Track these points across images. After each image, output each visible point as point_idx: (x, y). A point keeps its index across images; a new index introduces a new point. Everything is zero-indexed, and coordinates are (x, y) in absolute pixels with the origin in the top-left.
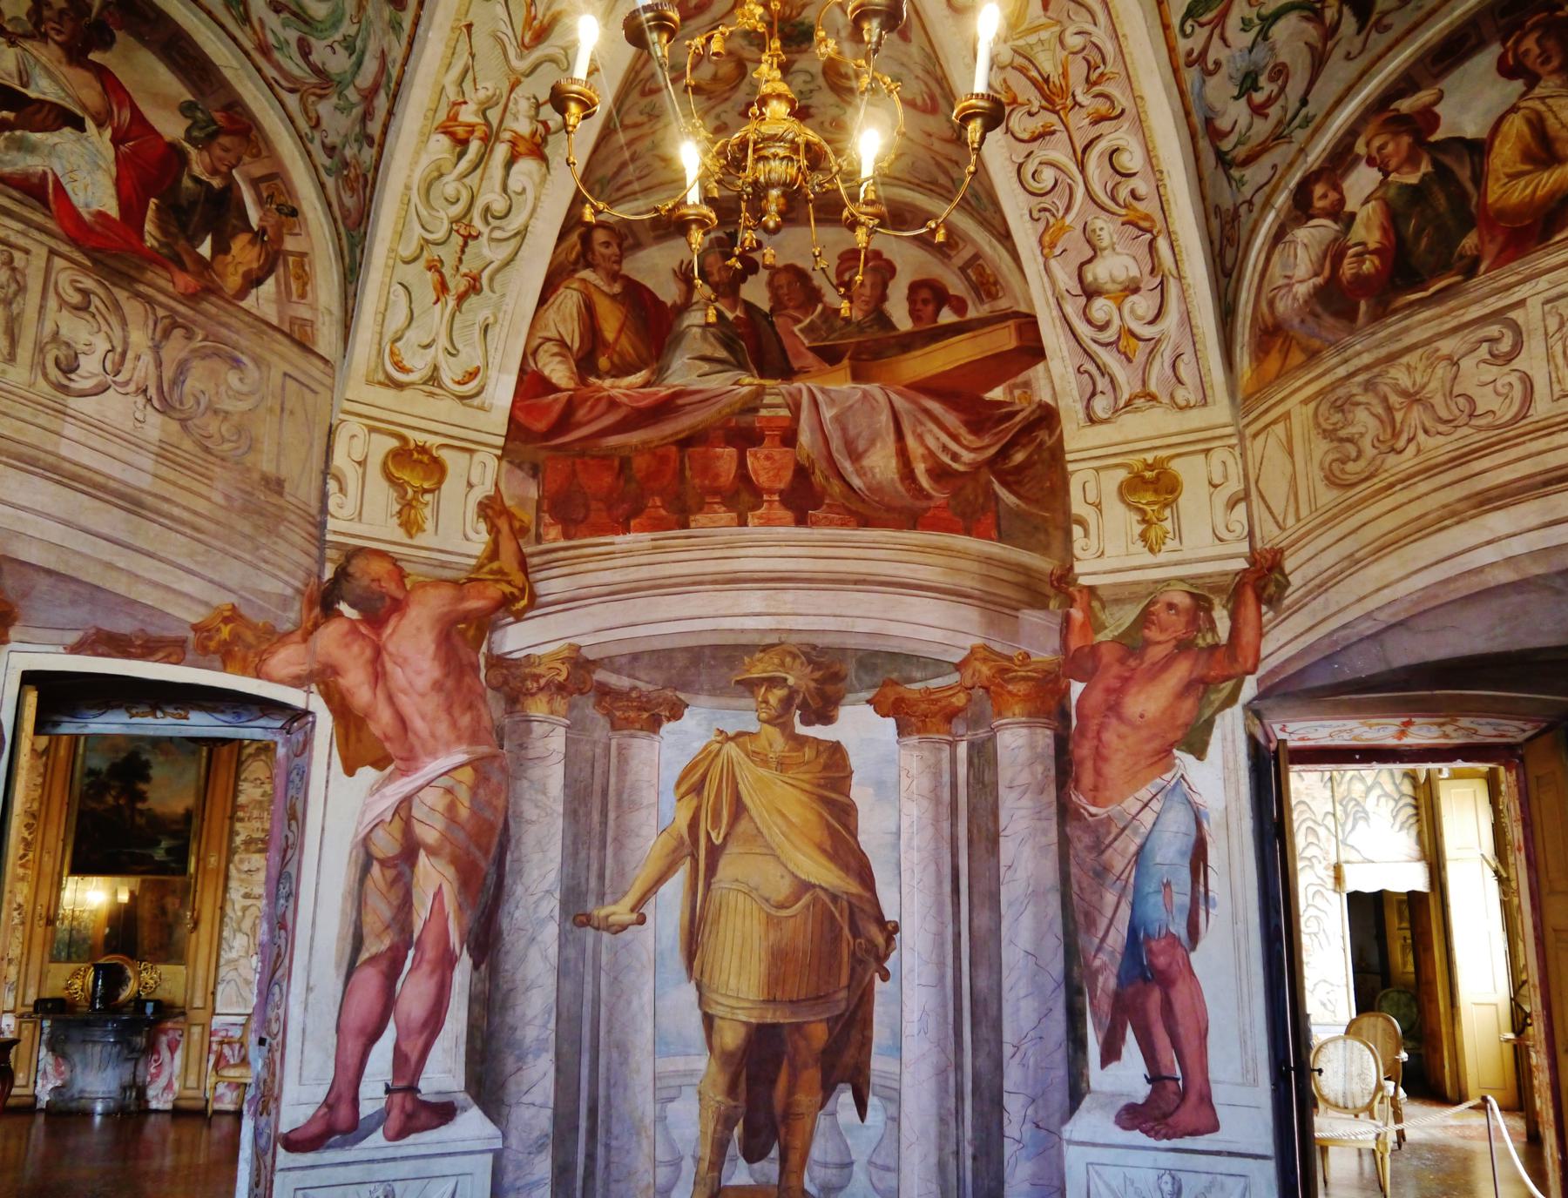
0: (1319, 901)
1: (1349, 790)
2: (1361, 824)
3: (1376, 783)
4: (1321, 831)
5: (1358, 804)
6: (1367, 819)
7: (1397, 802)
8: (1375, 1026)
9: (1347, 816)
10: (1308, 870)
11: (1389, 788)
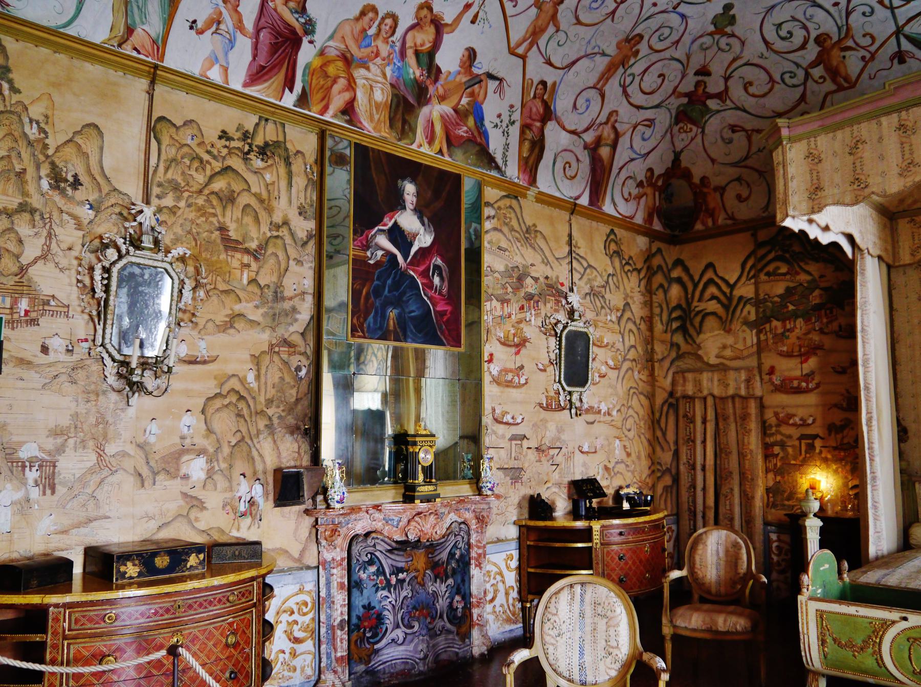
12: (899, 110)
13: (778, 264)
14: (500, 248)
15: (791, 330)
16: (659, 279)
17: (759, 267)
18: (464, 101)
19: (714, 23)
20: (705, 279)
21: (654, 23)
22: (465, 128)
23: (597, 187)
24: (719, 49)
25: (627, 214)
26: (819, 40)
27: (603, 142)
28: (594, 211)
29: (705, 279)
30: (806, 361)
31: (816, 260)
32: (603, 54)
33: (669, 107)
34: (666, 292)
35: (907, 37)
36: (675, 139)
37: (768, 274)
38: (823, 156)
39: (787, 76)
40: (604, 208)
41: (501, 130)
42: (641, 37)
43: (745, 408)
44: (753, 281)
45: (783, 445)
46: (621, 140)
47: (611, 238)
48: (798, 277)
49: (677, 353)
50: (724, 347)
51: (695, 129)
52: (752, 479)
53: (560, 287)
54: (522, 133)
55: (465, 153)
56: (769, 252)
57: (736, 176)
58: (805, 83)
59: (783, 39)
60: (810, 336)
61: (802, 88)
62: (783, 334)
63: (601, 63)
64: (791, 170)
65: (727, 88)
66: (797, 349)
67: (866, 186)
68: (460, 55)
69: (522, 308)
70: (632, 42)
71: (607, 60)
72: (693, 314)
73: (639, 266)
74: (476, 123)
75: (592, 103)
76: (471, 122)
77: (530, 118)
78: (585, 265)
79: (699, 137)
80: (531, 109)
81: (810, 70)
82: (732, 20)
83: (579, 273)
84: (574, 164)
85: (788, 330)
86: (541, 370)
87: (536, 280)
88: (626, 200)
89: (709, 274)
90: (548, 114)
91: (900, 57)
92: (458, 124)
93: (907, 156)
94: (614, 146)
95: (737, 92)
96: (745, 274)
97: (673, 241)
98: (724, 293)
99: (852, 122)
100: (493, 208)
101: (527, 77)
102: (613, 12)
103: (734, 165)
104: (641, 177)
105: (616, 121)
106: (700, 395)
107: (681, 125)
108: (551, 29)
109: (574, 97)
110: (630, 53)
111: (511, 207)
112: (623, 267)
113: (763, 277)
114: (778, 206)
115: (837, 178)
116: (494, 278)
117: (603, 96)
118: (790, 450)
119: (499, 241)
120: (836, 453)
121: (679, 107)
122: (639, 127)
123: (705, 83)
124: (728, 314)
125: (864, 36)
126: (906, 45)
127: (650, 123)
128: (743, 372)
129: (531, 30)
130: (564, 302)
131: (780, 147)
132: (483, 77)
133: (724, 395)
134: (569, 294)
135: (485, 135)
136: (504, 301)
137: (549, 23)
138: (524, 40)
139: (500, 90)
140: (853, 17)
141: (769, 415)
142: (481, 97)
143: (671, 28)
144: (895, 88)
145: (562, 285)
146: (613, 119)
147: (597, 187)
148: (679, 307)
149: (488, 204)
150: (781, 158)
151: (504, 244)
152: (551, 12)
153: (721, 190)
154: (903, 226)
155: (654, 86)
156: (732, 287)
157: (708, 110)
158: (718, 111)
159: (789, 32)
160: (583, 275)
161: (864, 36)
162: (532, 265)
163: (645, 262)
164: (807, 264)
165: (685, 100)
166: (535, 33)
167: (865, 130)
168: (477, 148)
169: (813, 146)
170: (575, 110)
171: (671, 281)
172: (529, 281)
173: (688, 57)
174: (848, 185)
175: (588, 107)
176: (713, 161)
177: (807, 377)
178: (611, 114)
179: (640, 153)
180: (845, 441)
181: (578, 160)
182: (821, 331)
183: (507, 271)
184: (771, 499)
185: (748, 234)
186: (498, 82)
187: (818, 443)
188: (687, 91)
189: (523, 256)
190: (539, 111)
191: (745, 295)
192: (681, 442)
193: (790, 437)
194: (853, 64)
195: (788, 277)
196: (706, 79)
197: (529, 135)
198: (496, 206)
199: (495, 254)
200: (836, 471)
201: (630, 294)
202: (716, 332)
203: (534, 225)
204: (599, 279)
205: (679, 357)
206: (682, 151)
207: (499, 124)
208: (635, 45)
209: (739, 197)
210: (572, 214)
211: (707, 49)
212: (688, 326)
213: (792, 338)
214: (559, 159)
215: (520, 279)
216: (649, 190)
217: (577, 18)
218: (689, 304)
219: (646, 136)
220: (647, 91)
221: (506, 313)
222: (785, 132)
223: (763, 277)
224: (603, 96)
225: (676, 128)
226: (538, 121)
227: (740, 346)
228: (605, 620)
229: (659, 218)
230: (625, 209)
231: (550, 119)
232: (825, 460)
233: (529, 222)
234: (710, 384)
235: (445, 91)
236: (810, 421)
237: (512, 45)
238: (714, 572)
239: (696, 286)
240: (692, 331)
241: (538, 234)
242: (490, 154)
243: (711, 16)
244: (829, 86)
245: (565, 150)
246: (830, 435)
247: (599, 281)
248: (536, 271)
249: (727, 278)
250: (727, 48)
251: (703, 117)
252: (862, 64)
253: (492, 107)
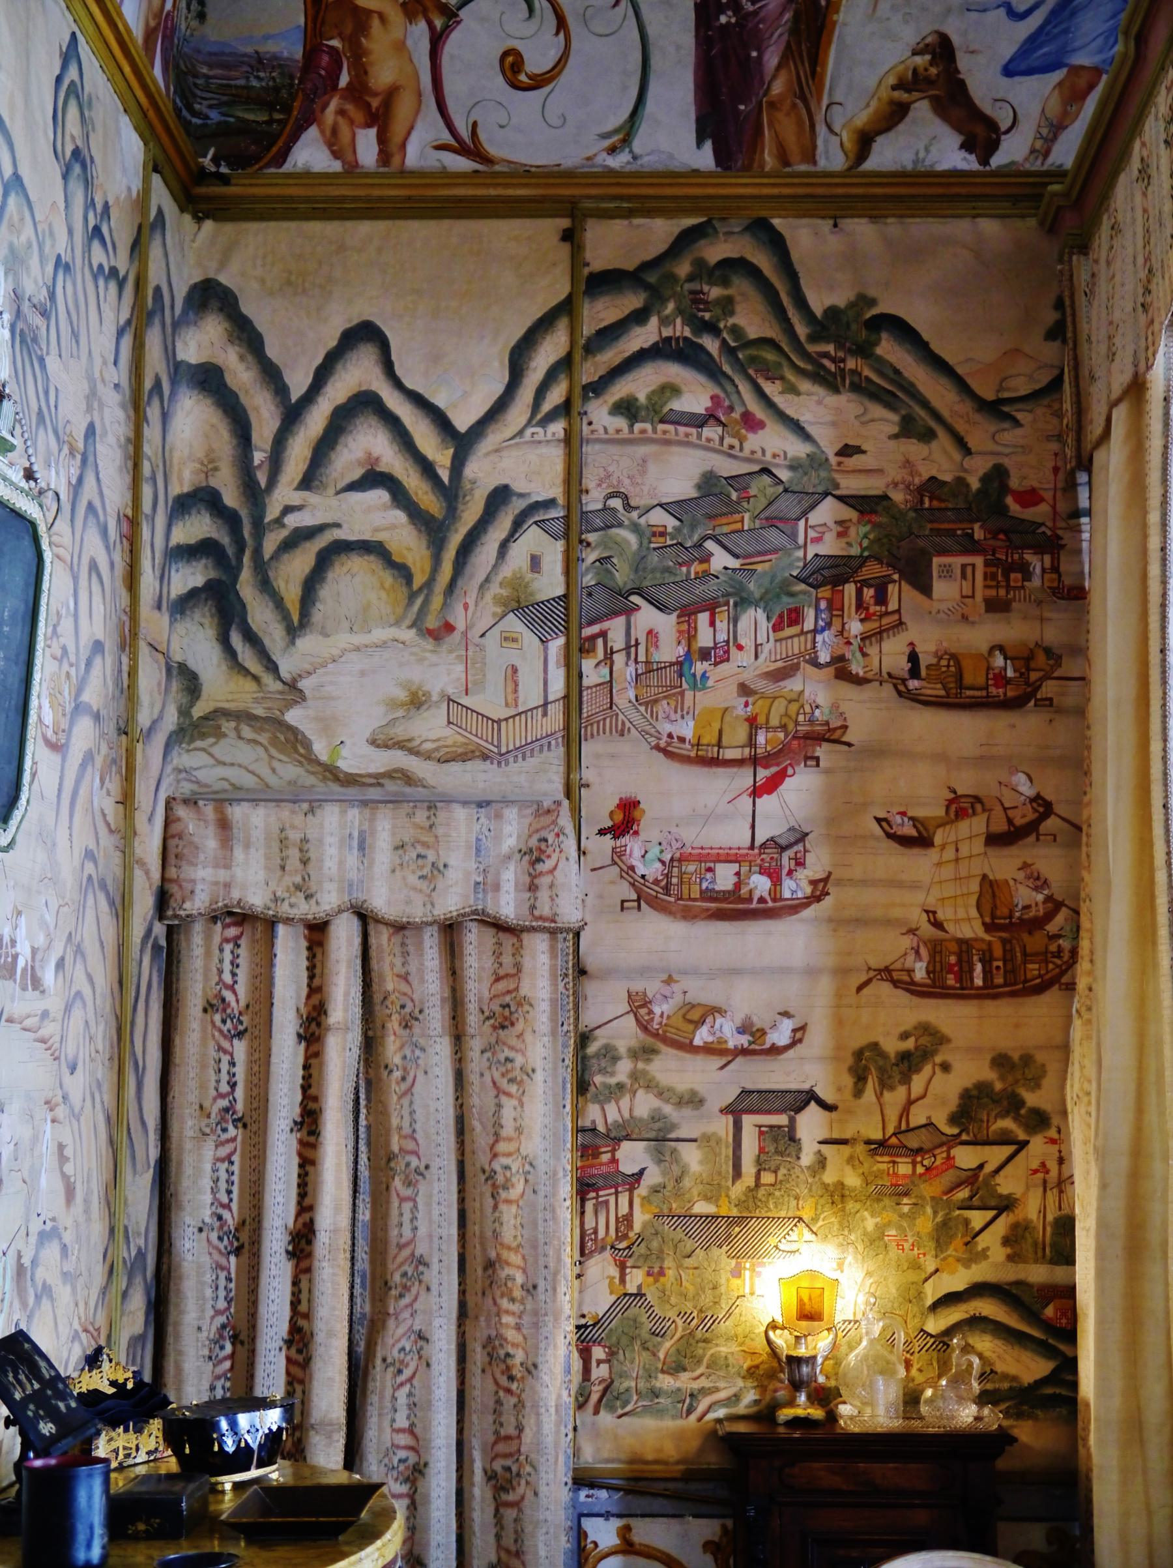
13: (673, 371)
15: (717, 655)
17: (589, 371)
20: (338, 391)
29: (338, 391)
30: (772, 785)
31: (830, 382)
37: (627, 409)
43: (507, 976)
44: (557, 428)
45: (661, 1138)
48: (754, 441)
49: (184, 712)
50: (417, 701)
52: (531, 1289)
56: (639, 317)
60: (794, 685)
62: (679, 666)
66: (741, 733)
72: (270, 545)
85: (705, 654)
89: (359, 373)
96: (526, 393)
97: (199, 196)
98: (427, 468)
106: (303, 909)
113: (600, 415)
118: (692, 1156)
120: (882, 1164)
128: (511, 813)
133: (417, 913)
141: (606, 1006)
148: (204, 498)
156: (463, 443)
164: (792, 390)
177: (776, 854)
180: (918, 1117)
182: (841, 671)
184: (600, 1372)
185: (551, 227)
187: (811, 1126)
191: (518, 486)
192: (186, 1125)
193: (694, 1100)
195: (711, 432)
200: (875, 1242)
202: (380, 634)
205: (193, 729)
209: (511, 65)
212: (246, 586)
213: (720, 689)
218: (255, 494)
227: (490, 701)
232: (837, 1195)
234: (352, 859)
236: (781, 1035)
240: (261, 615)
246: (858, 1093)
249: (440, 400)
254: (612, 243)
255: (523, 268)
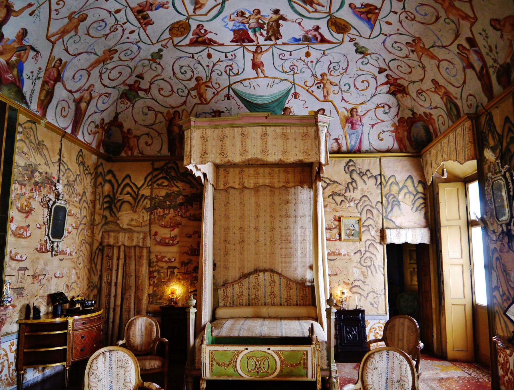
0: (371, 249)
1: (390, 190)
2: (396, 208)
3: (404, 186)
4: (375, 212)
5: (394, 197)
6: (399, 205)
7: (415, 196)
8: (403, 324)
9: (388, 203)
10: (366, 232)
11: (411, 189)
12: (242, 127)
14: (23, 152)
15: (167, 214)
16: (100, 180)
17: (154, 180)
18: (14, 58)
19: (152, 55)
20: (124, 183)
21: (125, 47)
22: (11, 75)
23: (77, 123)
24: (151, 68)
25: (89, 142)
26: (198, 79)
27: (83, 100)
28: (72, 137)
29: (124, 183)
31: (182, 181)
32: (96, 54)
33: (119, 89)
34: (102, 187)
35: (232, 89)
36: (118, 106)
37: (158, 185)
38: (208, 139)
39: (180, 91)
40: (78, 136)
41: (32, 81)
42: (116, 51)
43: (141, 252)
44: (150, 187)
45: (158, 272)
46: (92, 100)
47: (80, 154)
48: (173, 189)
49: (105, 221)
50: (132, 220)
51: (129, 103)
52: (142, 290)
53: (52, 179)
54: (43, 85)
55: (9, 90)
56: (160, 174)
57: (146, 133)
58: (187, 96)
59: (181, 73)
60: (176, 218)
61: (185, 98)
62: (163, 216)
63: (93, 58)
64: (194, 142)
65: (150, 88)
66: (169, 224)
67: (226, 157)
68: (18, 31)
69: (32, 190)
70: (111, 52)
71: (96, 57)
72: (116, 201)
73: (92, 172)
74: (18, 73)
75: (83, 77)
76: (15, 72)
77: (49, 78)
78: (66, 168)
79: (131, 108)
80: (50, 73)
81: (191, 91)
82: (161, 57)
83: (63, 172)
84: (67, 109)
85: (166, 214)
86: (38, 228)
87: (41, 173)
88: (89, 134)
89: (127, 181)
90: (59, 78)
91: (228, 97)
92: (7, 72)
93: (244, 147)
94: (88, 103)
95: (154, 91)
96: (146, 183)
97: (109, 160)
98: (134, 192)
99: (223, 127)
100: (22, 127)
101: (53, 55)
102: (107, 35)
103: (147, 126)
104: (98, 122)
105: (92, 90)
106: (117, 245)
107: (123, 100)
108: (73, 33)
109: (75, 72)
110: (108, 57)
111: (31, 128)
112: (84, 171)
113: (155, 186)
114: (185, 158)
115: (214, 150)
116: (18, 170)
117: (89, 75)
118: (162, 274)
119: (23, 147)
120: (184, 275)
121: (124, 90)
122: (103, 96)
123: (140, 82)
124: (135, 203)
125: (216, 83)
126: (231, 93)
127: (108, 95)
128: (141, 233)
129: (62, 30)
130: (54, 188)
131: (190, 130)
132: (28, 48)
133: (130, 245)
134: (57, 184)
135: (22, 82)
136: (22, 185)
137: (72, 29)
138: (57, 34)
139: (36, 58)
140: (213, 74)
141: (153, 256)
142: (23, 60)
143: (132, 51)
144: (242, 117)
145: (54, 178)
146: (91, 89)
147: (77, 123)
148: (108, 196)
149: (20, 125)
150: (189, 135)
151: (25, 150)
152: (75, 24)
153: (138, 138)
154: (221, 170)
155: (115, 77)
156: (139, 189)
157: (138, 96)
158: (143, 98)
159: (185, 71)
160: (64, 174)
161: (216, 83)
162: (40, 165)
163: (95, 169)
164: (177, 182)
165: (127, 88)
166: (63, 32)
167: (228, 131)
168: (16, 89)
169: (204, 133)
170: (73, 79)
171: (105, 181)
172: (37, 174)
173: (135, 67)
174: (218, 154)
175: (80, 79)
176: (136, 122)
177: (173, 238)
178: (90, 86)
179: (99, 110)
180: (189, 270)
181: (69, 107)
182: (181, 216)
183: (26, 166)
184: (151, 300)
185: (150, 163)
186: (35, 53)
187: (176, 271)
188: (130, 83)
189: (35, 159)
190: (54, 75)
191: (145, 194)
192: (104, 270)
193: (162, 268)
194: (209, 94)
195: (168, 187)
196: (141, 80)
197: (46, 87)
198: (23, 126)
199: (20, 156)
200: (183, 285)
201: (86, 187)
202: (128, 212)
203: (43, 141)
204: (72, 176)
205: (106, 223)
206: (120, 113)
207: (31, 77)
208: (112, 54)
209: (146, 143)
210: (63, 137)
211: (145, 66)
212: (113, 207)
213: (168, 217)
214: (59, 105)
215: (33, 173)
216: (100, 130)
217: (88, 32)
218: (114, 195)
219: (105, 102)
220: (112, 78)
221: (23, 192)
222: (193, 123)
223: (155, 186)
224: (89, 75)
225: (120, 101)
226: (53, 80)
227: (141, 220)
228: (124, 369)
229: (103, 147)
230: (88, 139)
231: (59, 81)
232: (179, 279)
233: (40, 139)
234: (123, 239)
235: (4, 49)
236: (173, 260)
237: (49, 35)
238: (139, 339)
239: (119, 186)
240: (115, 210)
241: (44, 147)
242: (23, 94)
243: (151, 52)
244: (197, 101)
245: (64, 100)
246: (182, 267)
247: (72, 178)
248: (41, 169)
249: (136, 184)
250: (155, 69)
251: (135, 98)
252: (213, 95)
253: (30, 67)
254: (157, 165)
255: (146, 168)
